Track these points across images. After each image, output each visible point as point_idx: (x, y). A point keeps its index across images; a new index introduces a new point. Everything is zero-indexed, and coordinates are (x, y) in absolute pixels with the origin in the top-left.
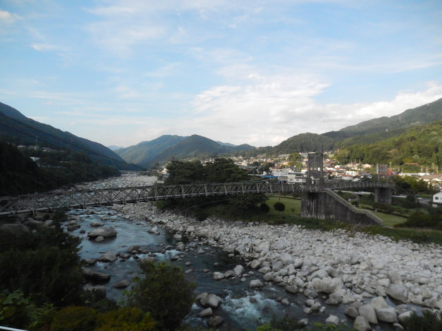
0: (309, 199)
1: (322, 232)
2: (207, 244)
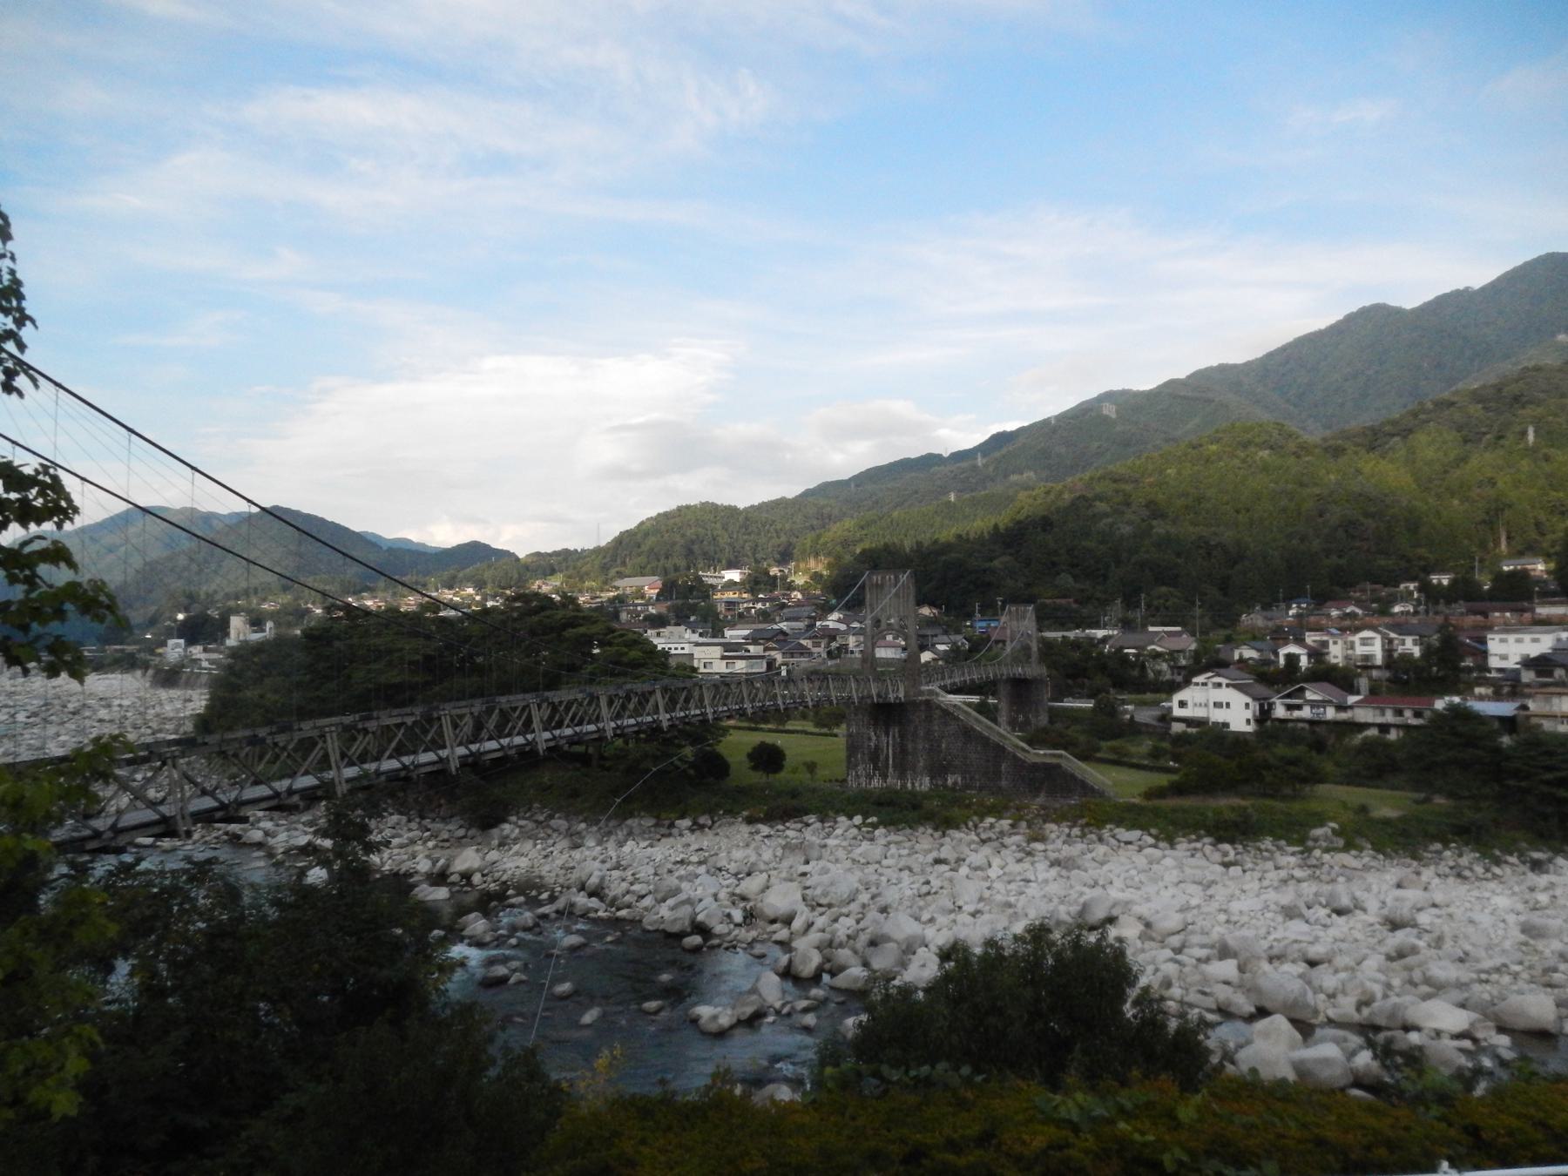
0: (876, 725)
1: (940, 833)
2: (568, 913)
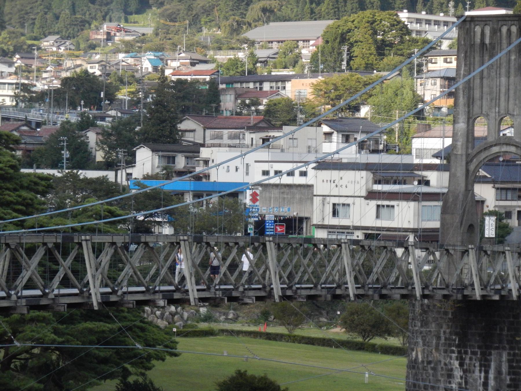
0: (462, 345)
